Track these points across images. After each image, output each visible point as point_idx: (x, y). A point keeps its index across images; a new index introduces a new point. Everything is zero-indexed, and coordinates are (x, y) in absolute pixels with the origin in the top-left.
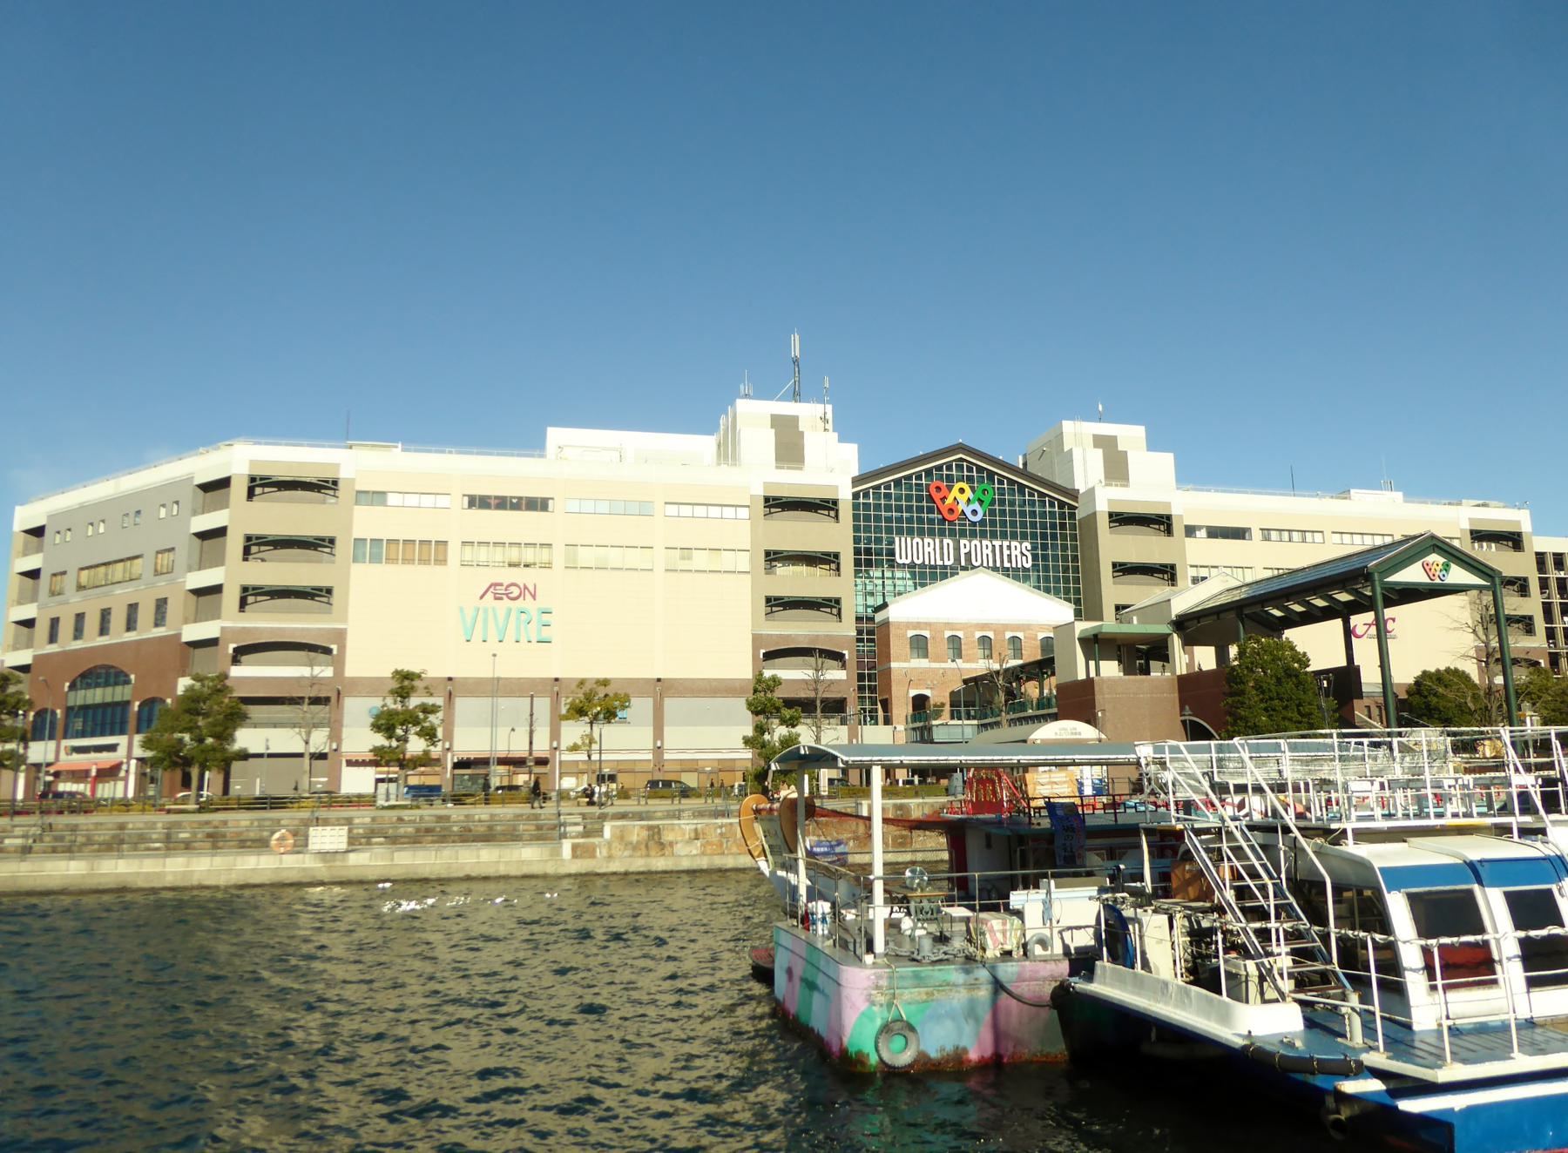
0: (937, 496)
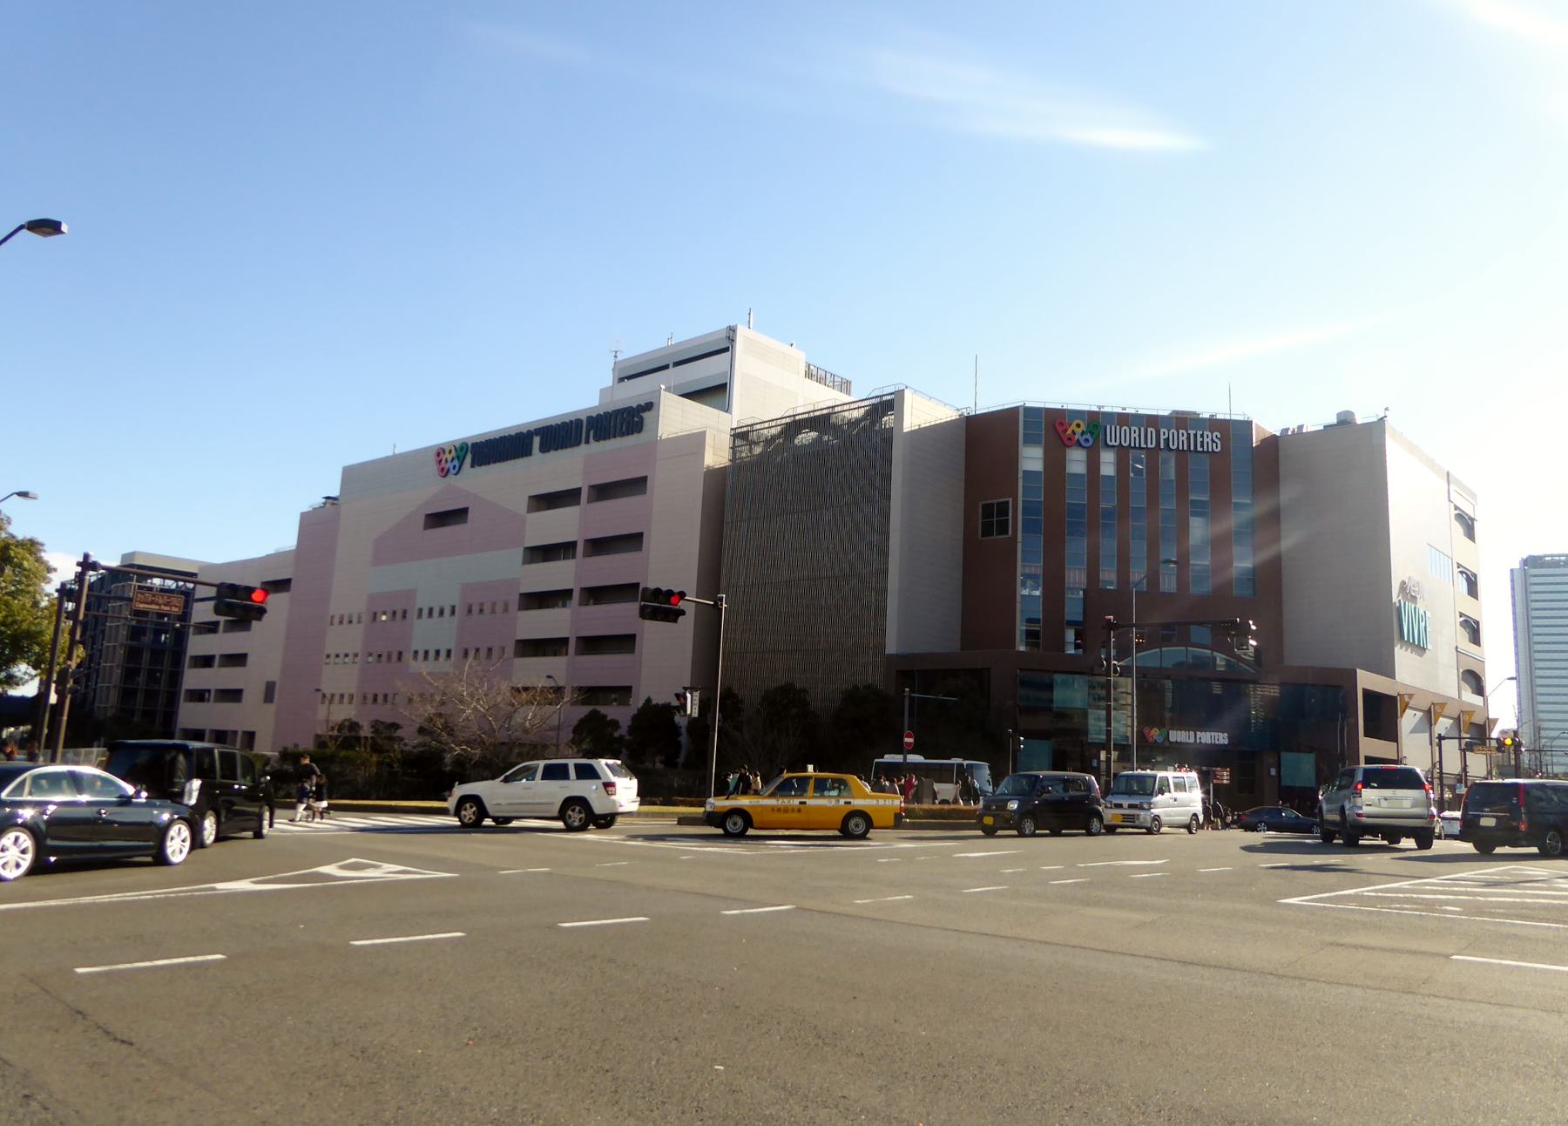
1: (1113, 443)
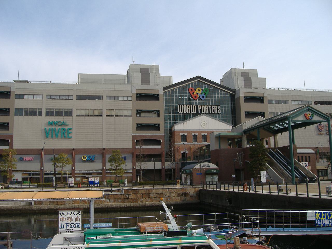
0: (191, 92)
1: (181, 112)
